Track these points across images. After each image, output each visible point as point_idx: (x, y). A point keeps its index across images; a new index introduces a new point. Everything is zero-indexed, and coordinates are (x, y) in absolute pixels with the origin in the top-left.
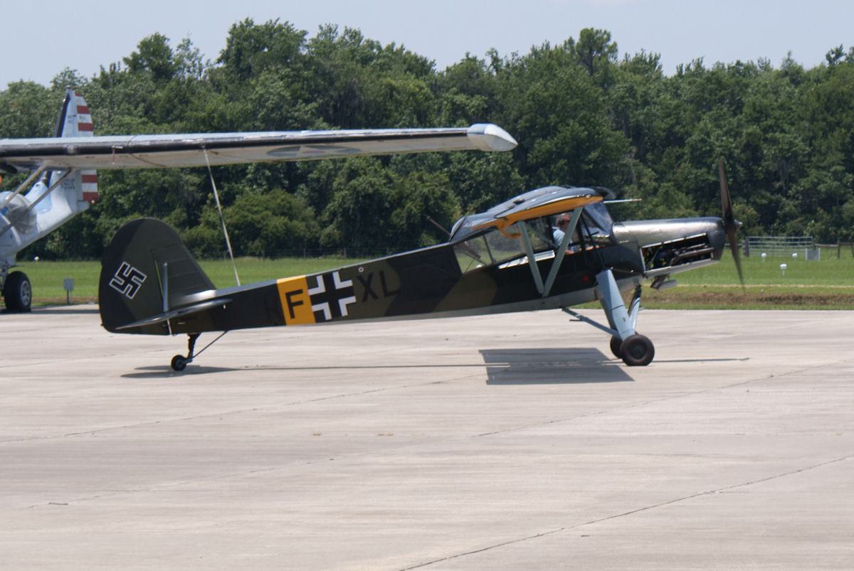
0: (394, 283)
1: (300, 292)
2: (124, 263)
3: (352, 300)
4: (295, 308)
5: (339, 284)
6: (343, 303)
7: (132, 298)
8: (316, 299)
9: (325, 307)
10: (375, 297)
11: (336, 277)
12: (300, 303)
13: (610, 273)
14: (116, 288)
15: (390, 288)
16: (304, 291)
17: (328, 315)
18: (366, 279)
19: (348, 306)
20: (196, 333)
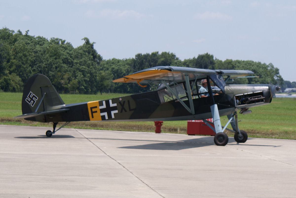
0: (133, 106)
1: (96, 107)
3: (116, 111)
4: (94, 114)
5: (112, 105)
6: (113, 113)
8: (102, 111)
9: (105, 114)
10: (126, 111)
11: (111, 101)
12: (96, 112)
13: (216, 106)
15: (132, 108)
16: (97, 107)
17: (107, 118)
18: (122, 104)
19: (114, 114)
20: (56, 122)
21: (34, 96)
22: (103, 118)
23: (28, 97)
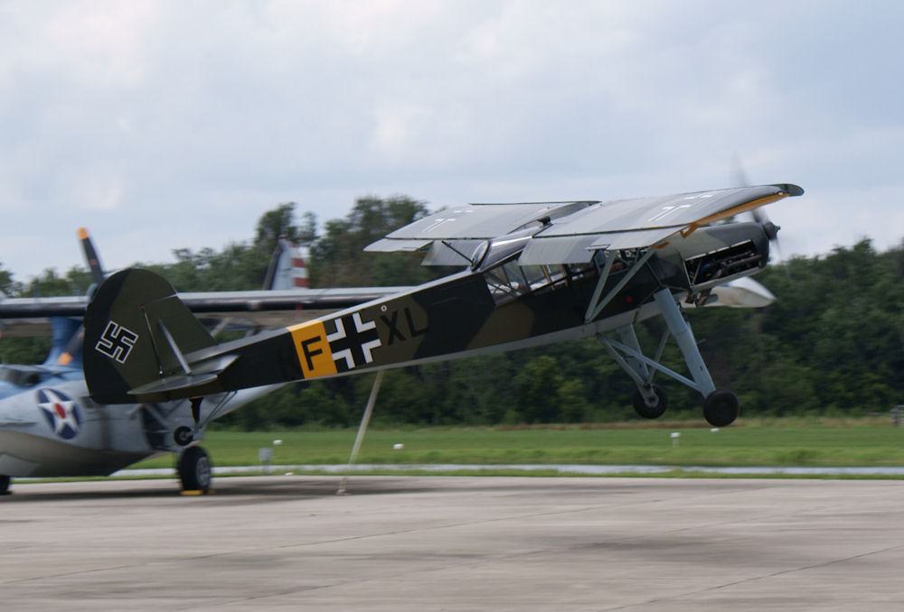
0: (421, 321)
1: (318, 339)
3: (376, 343)
4: (313, 358)
5: (361, 327)
6: (366, 348)
8: (336, 346)
9: (347, 354)
10: (402, 338)
11: (357, 318)
12: (319, 352)
15: (416, 329)
16: (322, 338)
17: (351, 364)
18: (390, 318)
19: (371, 350)
22: (341, 364)
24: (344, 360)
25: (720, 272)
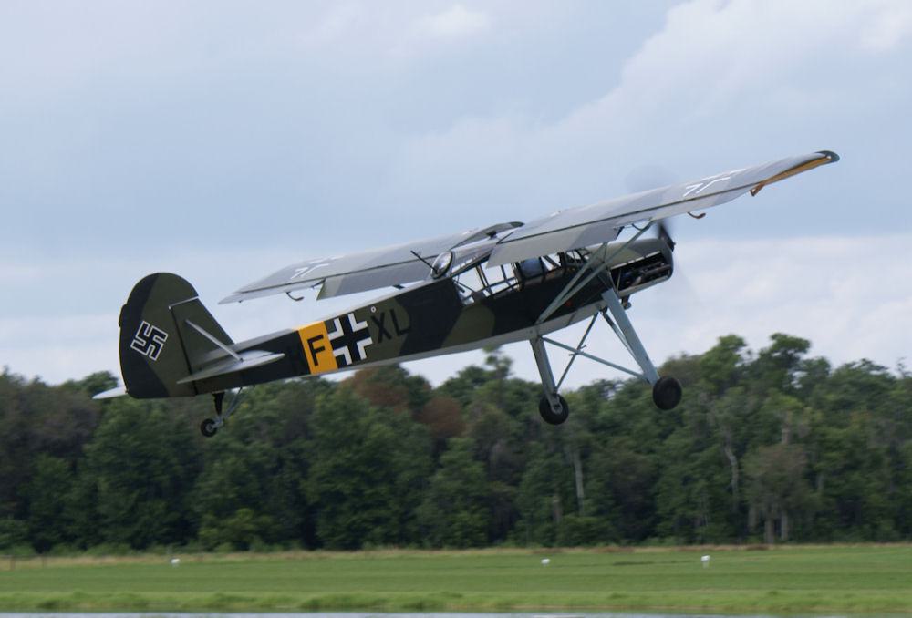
0: (404, 323)
1: (320, 337)
2: (144, 322)
3: (369, 341)
4: (317, 355)
5: (356, 327)
6: (361, 345)
7: (155, 359)
8: (336, 344)
9: (345, 351)
10: (389, 337)
11: (352, 318)
12: (322, 349)
14: (138, 350)
15: (401, 328)
17: (349, 360)
18: (378, 318)
21: (154, 332)
23: (137, 336)
24: (343, 356)
25: (639, 279)
